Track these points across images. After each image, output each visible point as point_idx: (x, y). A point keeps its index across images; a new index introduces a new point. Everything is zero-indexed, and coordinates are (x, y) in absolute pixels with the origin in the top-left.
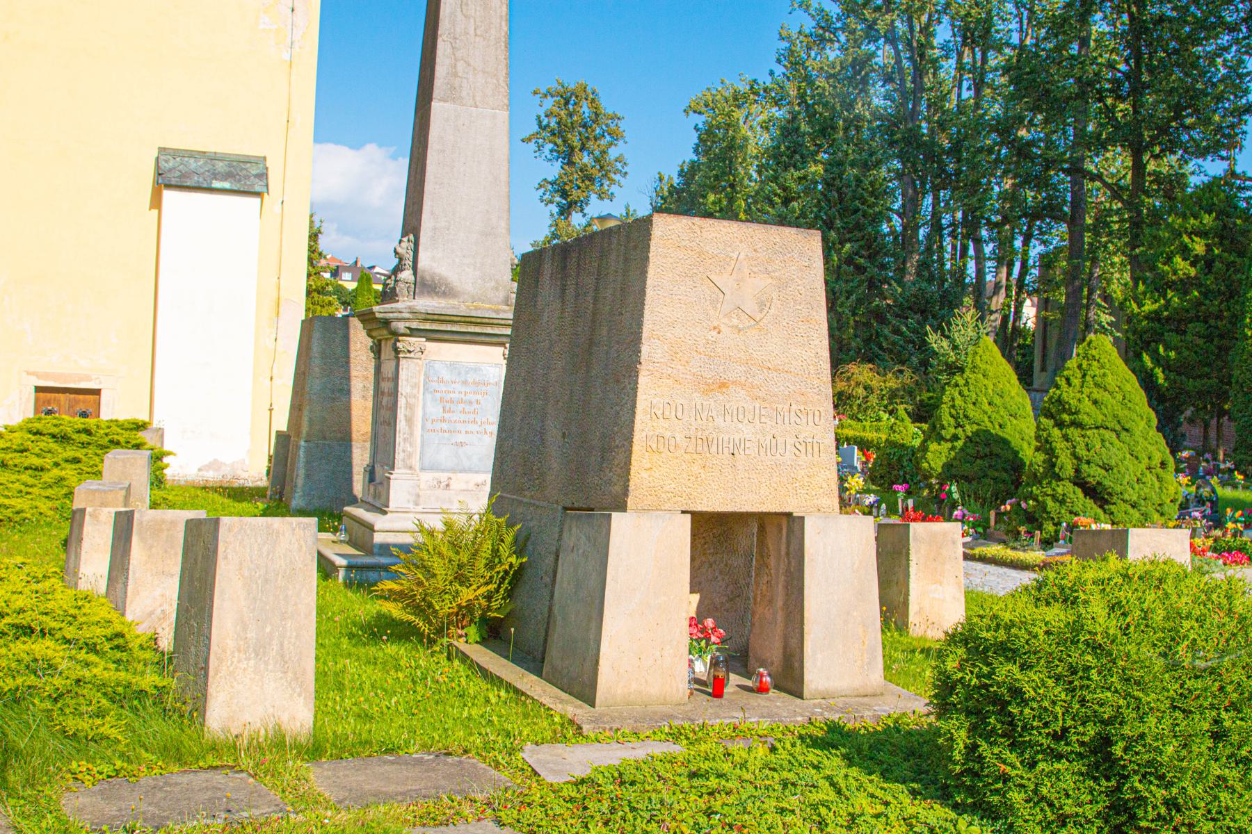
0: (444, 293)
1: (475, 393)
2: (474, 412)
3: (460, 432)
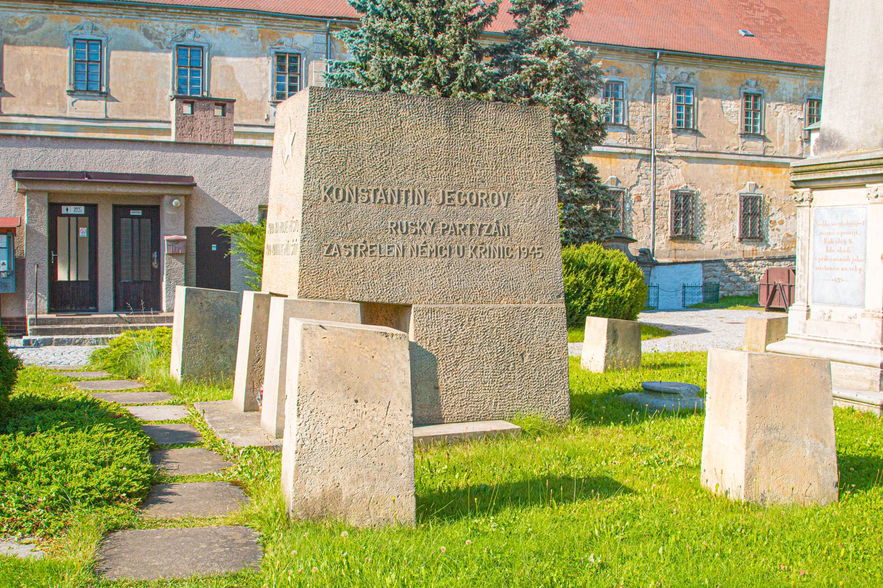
0: (837, 145)
1: (848, 233)
2: (848, 251)
3: (838, 269)
